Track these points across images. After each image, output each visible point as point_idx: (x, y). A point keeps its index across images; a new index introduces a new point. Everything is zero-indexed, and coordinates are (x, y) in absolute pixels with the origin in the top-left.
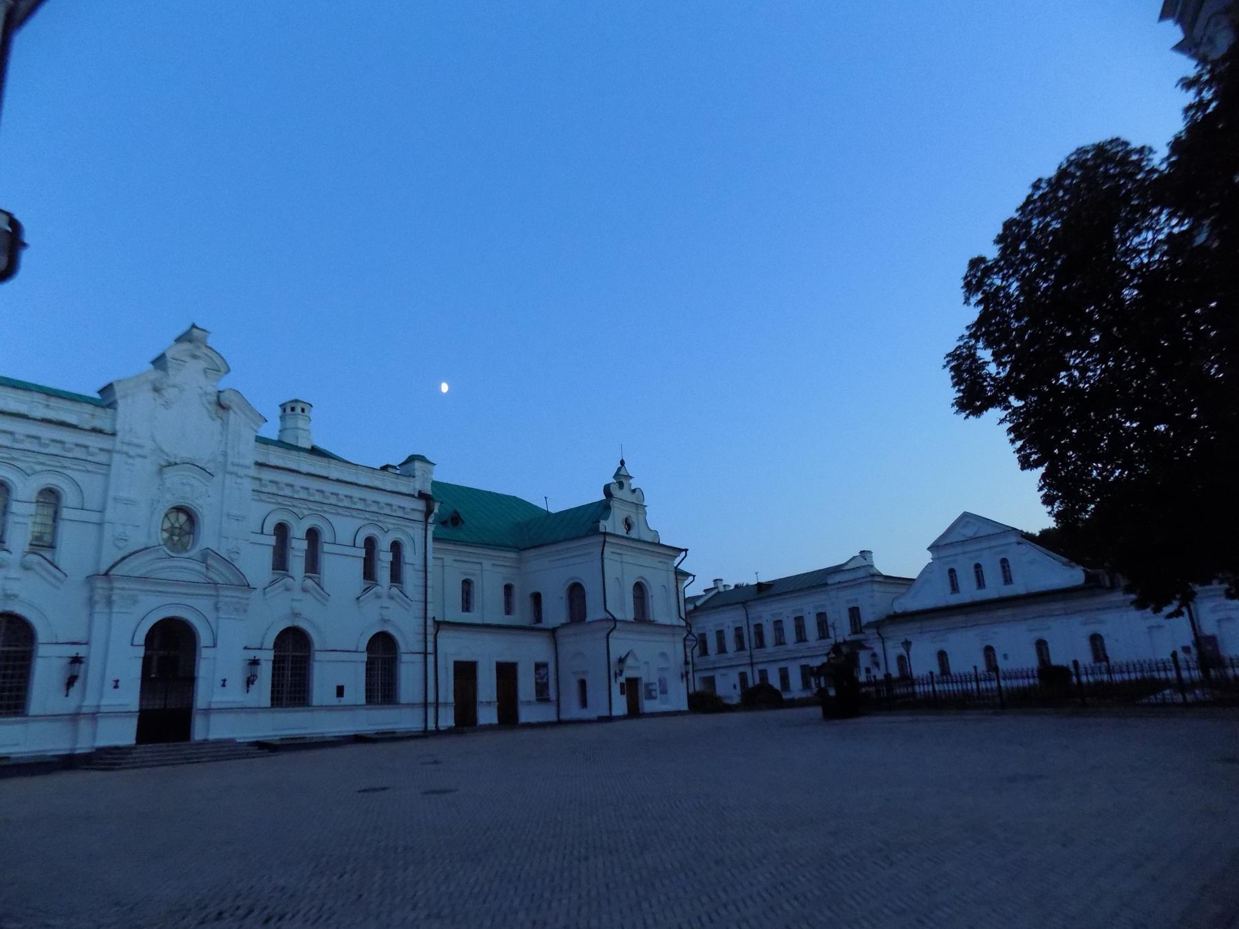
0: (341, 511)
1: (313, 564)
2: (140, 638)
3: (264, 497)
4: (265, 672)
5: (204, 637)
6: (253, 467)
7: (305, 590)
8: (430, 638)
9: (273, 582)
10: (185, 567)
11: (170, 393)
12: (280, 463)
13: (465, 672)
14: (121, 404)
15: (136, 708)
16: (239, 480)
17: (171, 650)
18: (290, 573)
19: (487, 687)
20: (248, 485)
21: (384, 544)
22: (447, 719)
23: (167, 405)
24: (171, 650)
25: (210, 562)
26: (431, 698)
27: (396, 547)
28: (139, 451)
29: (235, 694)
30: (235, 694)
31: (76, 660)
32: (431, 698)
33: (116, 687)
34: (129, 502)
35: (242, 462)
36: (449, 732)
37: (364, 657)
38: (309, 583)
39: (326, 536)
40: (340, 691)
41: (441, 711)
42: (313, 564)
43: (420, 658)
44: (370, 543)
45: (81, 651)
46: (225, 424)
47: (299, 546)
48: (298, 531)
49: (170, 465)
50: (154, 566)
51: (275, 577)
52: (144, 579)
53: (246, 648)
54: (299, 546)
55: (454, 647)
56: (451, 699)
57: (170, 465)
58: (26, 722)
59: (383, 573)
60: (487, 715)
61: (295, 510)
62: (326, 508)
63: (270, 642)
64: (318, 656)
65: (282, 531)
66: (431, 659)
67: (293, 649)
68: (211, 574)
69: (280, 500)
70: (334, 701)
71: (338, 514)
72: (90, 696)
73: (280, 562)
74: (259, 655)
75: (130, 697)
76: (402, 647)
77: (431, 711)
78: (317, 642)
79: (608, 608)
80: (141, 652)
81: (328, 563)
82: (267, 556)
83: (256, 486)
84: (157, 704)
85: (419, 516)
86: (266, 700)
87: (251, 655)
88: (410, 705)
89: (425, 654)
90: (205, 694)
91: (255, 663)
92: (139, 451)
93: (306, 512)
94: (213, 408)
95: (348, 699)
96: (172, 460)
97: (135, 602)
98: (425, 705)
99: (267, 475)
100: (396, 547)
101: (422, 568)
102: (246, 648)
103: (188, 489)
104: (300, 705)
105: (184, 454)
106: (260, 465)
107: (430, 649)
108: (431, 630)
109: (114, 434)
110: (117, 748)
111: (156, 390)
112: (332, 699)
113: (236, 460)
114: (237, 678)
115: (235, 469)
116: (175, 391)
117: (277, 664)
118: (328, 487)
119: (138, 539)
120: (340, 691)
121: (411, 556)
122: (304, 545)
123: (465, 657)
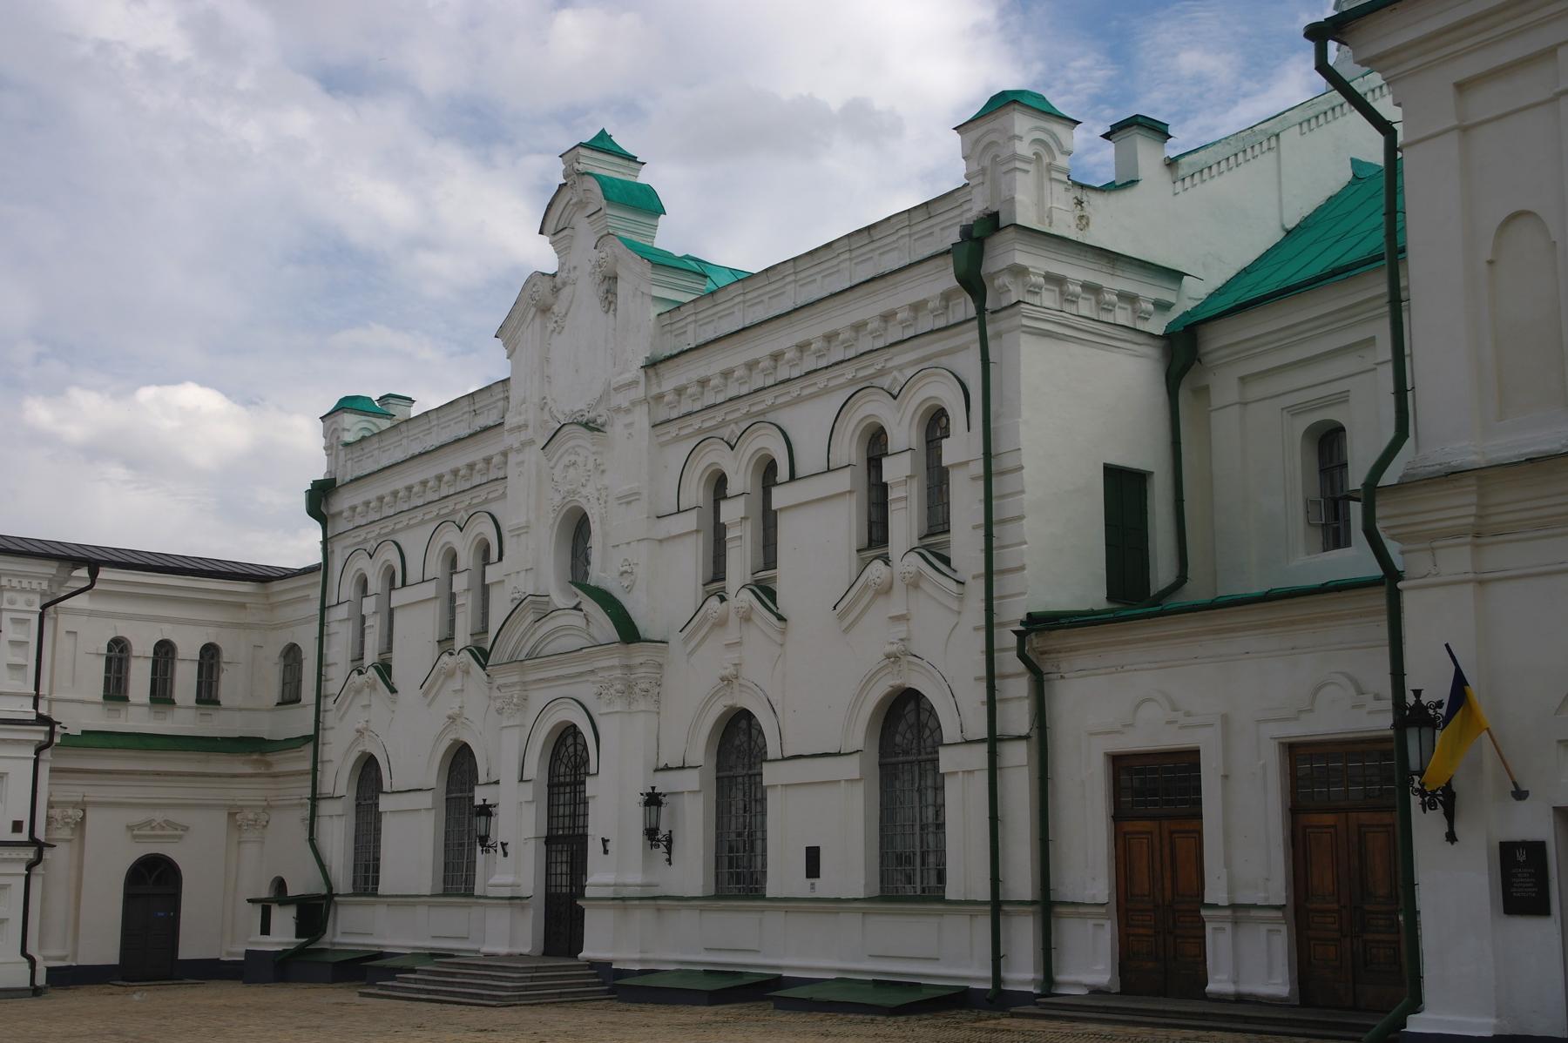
0: (794, 390)
4: (693, 822)
8: (1017, 687)
13: (1157, 793)
16: (628, 419)
19: (1245, 846)
20: (641, 418)
22: (1090, 961)
26: (1021, 883)
36: (1094, 1006)
43: (980, 754)
44: (876, 443)
53: (667, 768)
55: (1118, 703)
58: (469, 906)
59: (904, 524)
60: (1250, 962)
62: (768, 398)
63: (699, 750)
66: (1017, 757)
71: (799, 400)
74: (663, 783)
77: (1022, 934)
79: (1389, 433)
88: (966, 905)
89: (994, 741)
98: (997, 906)
99: (671, 379)
101: (979, 468)
102: (667, 768)
103: (571, 470)
104: (747, 898)
106: (652, 365)
107: (1017, 717)
108: (1009, 661)
121: (960, 447)
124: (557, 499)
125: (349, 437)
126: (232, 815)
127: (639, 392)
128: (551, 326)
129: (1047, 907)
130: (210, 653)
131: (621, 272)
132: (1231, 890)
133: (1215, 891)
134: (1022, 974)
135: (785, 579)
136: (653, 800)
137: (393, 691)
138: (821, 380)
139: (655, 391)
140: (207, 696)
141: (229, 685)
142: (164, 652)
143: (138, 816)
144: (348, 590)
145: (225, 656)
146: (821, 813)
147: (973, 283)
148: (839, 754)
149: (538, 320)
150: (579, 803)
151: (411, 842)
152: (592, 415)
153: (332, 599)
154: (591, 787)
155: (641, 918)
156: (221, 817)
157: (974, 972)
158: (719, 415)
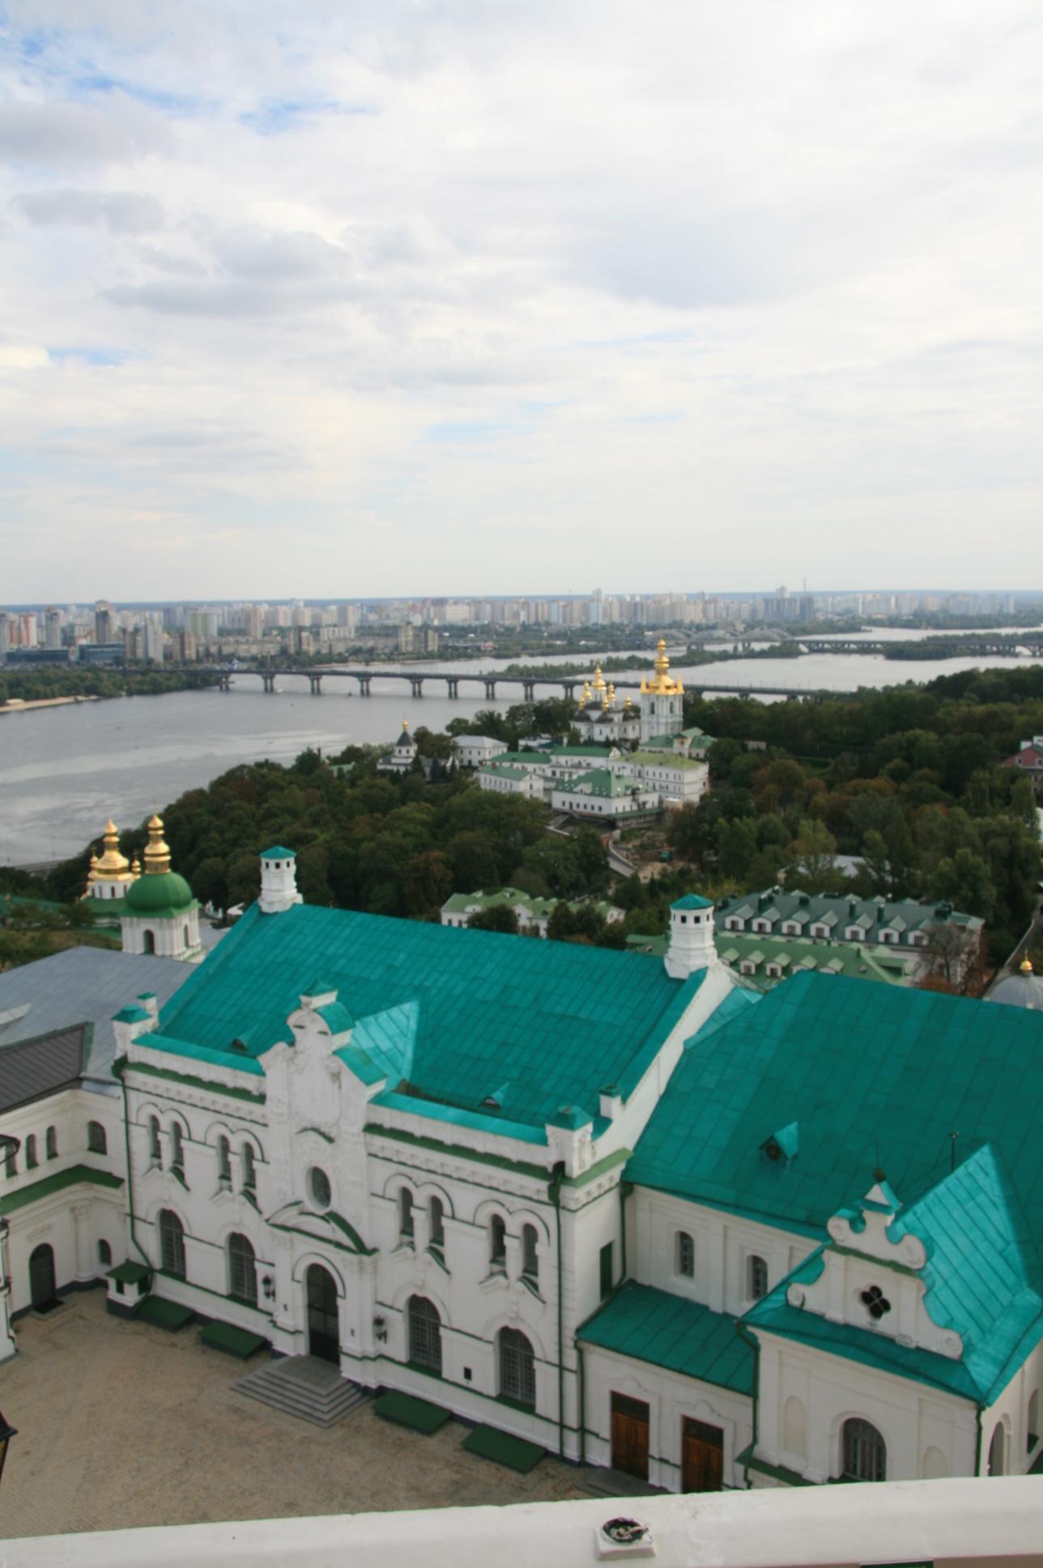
2: (301, 1275)
17: (322, 1291)
21: (513, 1226)
22: (601, 1455)
24: (322, 1291)
26: (572, 1420)
27: (530, 1234)
31: (267, 1281)
32: (572, 1420)
40: (468, 1374)
41: (591, 1439)
42: (438, 1236)
48: (421, 1198)
53: (381, 1304)
56: (606, 1432)
63: (402, 1302)
65: (407, 1198)
67: (423, 1317)
70: (462, 1380)
73: (407, 1227)
76: (538, 1353)
77: (572, 1440)
78: (444, 1320)
85: (545, 1197)
86: (402, 1354)
89: (561, 1368)
99: (379, 1142)
100: (530, 1234)
102: (381, 1304)
105: (318, 1120)
107: (571, 1361)
120: (468, 1374)
121: (545, 1251)
123: (629, 1390)
125: (134, 1037)
126: (73, 1210)
129: (583, 1430)
130: (51, 1132)
132: (660, 1451)
133: (653, 1450)
134: (572, 1453)
135: (448, 1250)
136: (379, 1322)
137: (188, 1189)
140: (52, 1154)
141: (60, 1147)
142: (31, 1139)
143: (30, 1230)
144: (144, 1119)
145: (58, 1131)
146: (470, 1355)
147: (555, 1200)
148: (480, 1339)
150: (333, 1312)
151: (208, 1266)
153: (133, 1119)
154: (339, 1301)
156: (67, 1212)
157: (553, 1446)
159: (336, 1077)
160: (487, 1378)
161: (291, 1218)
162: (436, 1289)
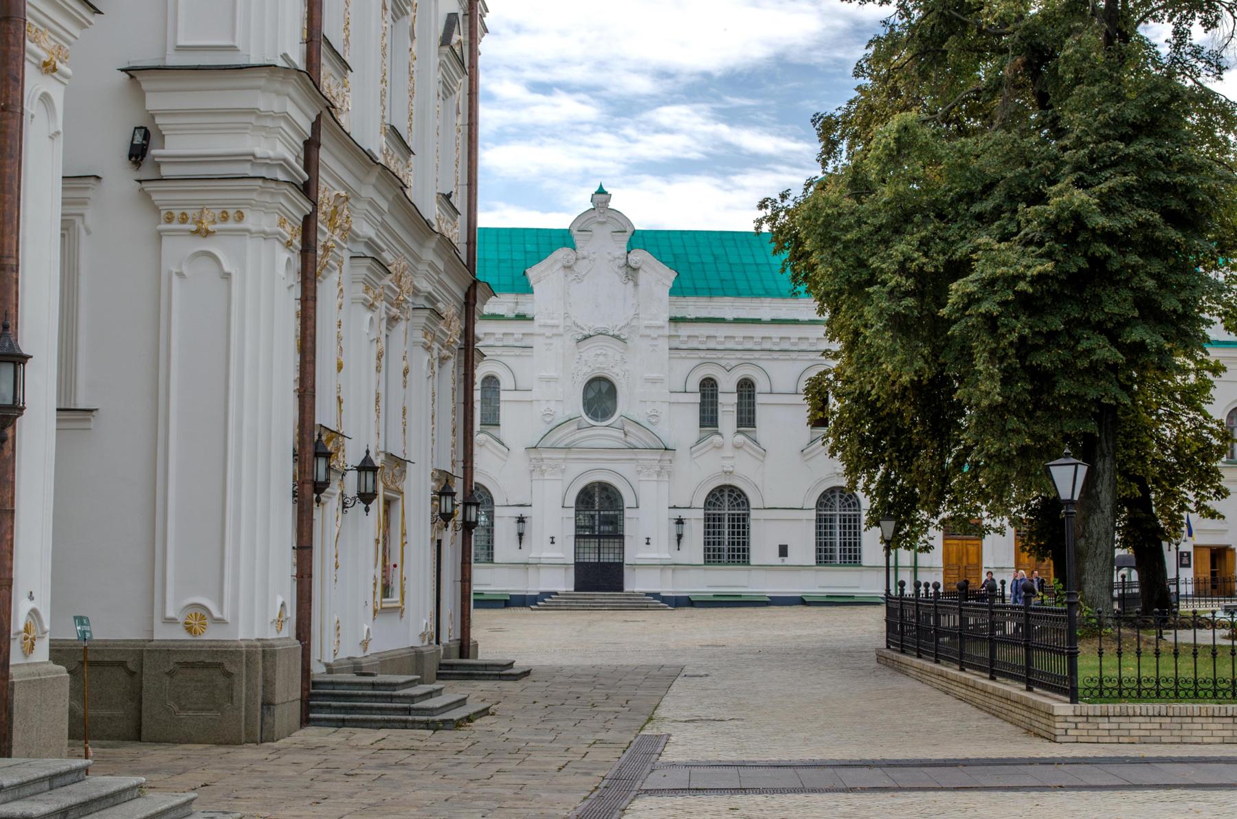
0: (776, 355)
1: (746, 418)
2: (571, 501)
3: (683, 354)
5: (628, 500)
6: (667, 325)
7: (737, 447)
9: (698, 442)
10: (603, 433)
11: (581, 267)
12: (704, 314)
14: (536, 288)
15: (571, 560)
16: (655, 342)
17: (600, 510)
18: (720, 429)
20: (664, 345)
23: (579, 279)
24: (600, 510)
25: (626, 428)
28: (555, 331)
29: (662, 551)
30: (662, 551)
31: (521, 520)
33: (553, 543)
34: (548, 380)
35: (654, 323)
37: (813, 515)
38: (741, 438)
39: (761, 385)
40: (783, 551)
42: (746, 418)
45: (524, 512)
46: (636, 285)
47: (728, 403)
49: (586, 338)
50: (577, 436)
51: (704, 434)
52: (568, 448)
53: (675, 507)
54: (728, 403)
57: (586, 338)
61: (723, 363)
62: (757, 355)
63: (700, 502)
64: (754, 514)
65: (709, 388)
68: (628, 439)
69: (702, 354)
70: (778, 561)
72: (538, 549)
73: (708, 418)
74: (684, 514)
75: (565, 552)
78: (754, 503)
80: (572, 513)
81: (761, 414)
82: (694, 414)
83: (676, 344)
84: (592, 558)
87: (677, 514)
90: (634, 552)
91: (680, 522)
92: (555, 331)
93: (734, 363)
94: (622, 272)
95: (793, 558)
96: (586, 333)
97: (563, 471)
99: (685, 330)
102: (675, 507)
103: (601, 358)
106: (674, 320)
109: (532, 319)
110: (556, 593)
111: (568, 268)
112: (775, 559)
113: (647, 323)
114: (663, 533)
115: (648, 332)
116: (586, 261)
117: (712, 523)
118: (758, 332)
119: (561, 415)
120: (783, 551)
122: (734, 398)
124: (586, 369)
127: (666, 332)
128: (573, 277)
131: (644, 267)
138: (794, 355)
139: (674, 333)
149: (562, 273)
152: (616, 333)
154: (627, 513)
155: (669, 573)
158: (720, 355)
159: (632, 271)
160: (804, 548)
161: (565, 436)
162: (744, 471)
